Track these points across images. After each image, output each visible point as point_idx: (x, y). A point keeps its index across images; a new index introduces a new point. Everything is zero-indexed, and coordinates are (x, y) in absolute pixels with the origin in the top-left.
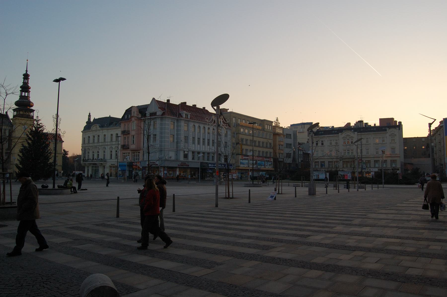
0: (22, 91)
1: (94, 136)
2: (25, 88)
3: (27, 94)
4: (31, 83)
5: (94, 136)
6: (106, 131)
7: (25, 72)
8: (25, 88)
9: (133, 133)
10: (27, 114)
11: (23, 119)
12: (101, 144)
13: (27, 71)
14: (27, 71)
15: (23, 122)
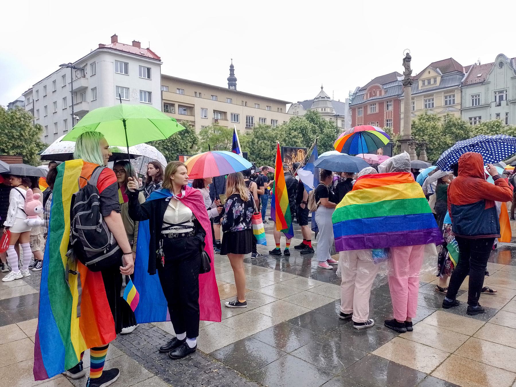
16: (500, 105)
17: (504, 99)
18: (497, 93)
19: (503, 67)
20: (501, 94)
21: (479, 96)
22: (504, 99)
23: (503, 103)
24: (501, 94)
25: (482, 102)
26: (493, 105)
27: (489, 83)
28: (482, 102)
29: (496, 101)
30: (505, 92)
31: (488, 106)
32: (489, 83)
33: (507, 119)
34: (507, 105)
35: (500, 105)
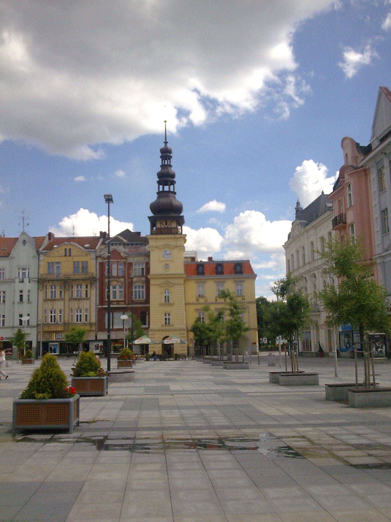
0: (159, 183)
1: (298, 251)
2: (166, 178)
3: (172, 187)
4: (176, 167)
5: (298, 251)
6: (312, 232)
7: (163, 146)
8: (166, 178)
9: (350, 218)
10: (169, 226)
11: (159, 236)
12: (308, 268)
13: (166, 143)
14: (166, 143)
15: (160, 243)
16: (22, 282)
17: (27, 276)
18: (21, 269)
19: (26, 245)
20: (24, 271)
21: (4, 270)
22: (27, 276)
23: (26, 280)
24: (24, 271)
25: (7, 276)
26: (17, 281)
27: (13, 258)
28: (7, 276)
29: (19, 277)
30: (27, 270)
31: (12, 281)
32: (13, 258)
33: (29, 295)
34: (29, 282)
35: (22, 282)
